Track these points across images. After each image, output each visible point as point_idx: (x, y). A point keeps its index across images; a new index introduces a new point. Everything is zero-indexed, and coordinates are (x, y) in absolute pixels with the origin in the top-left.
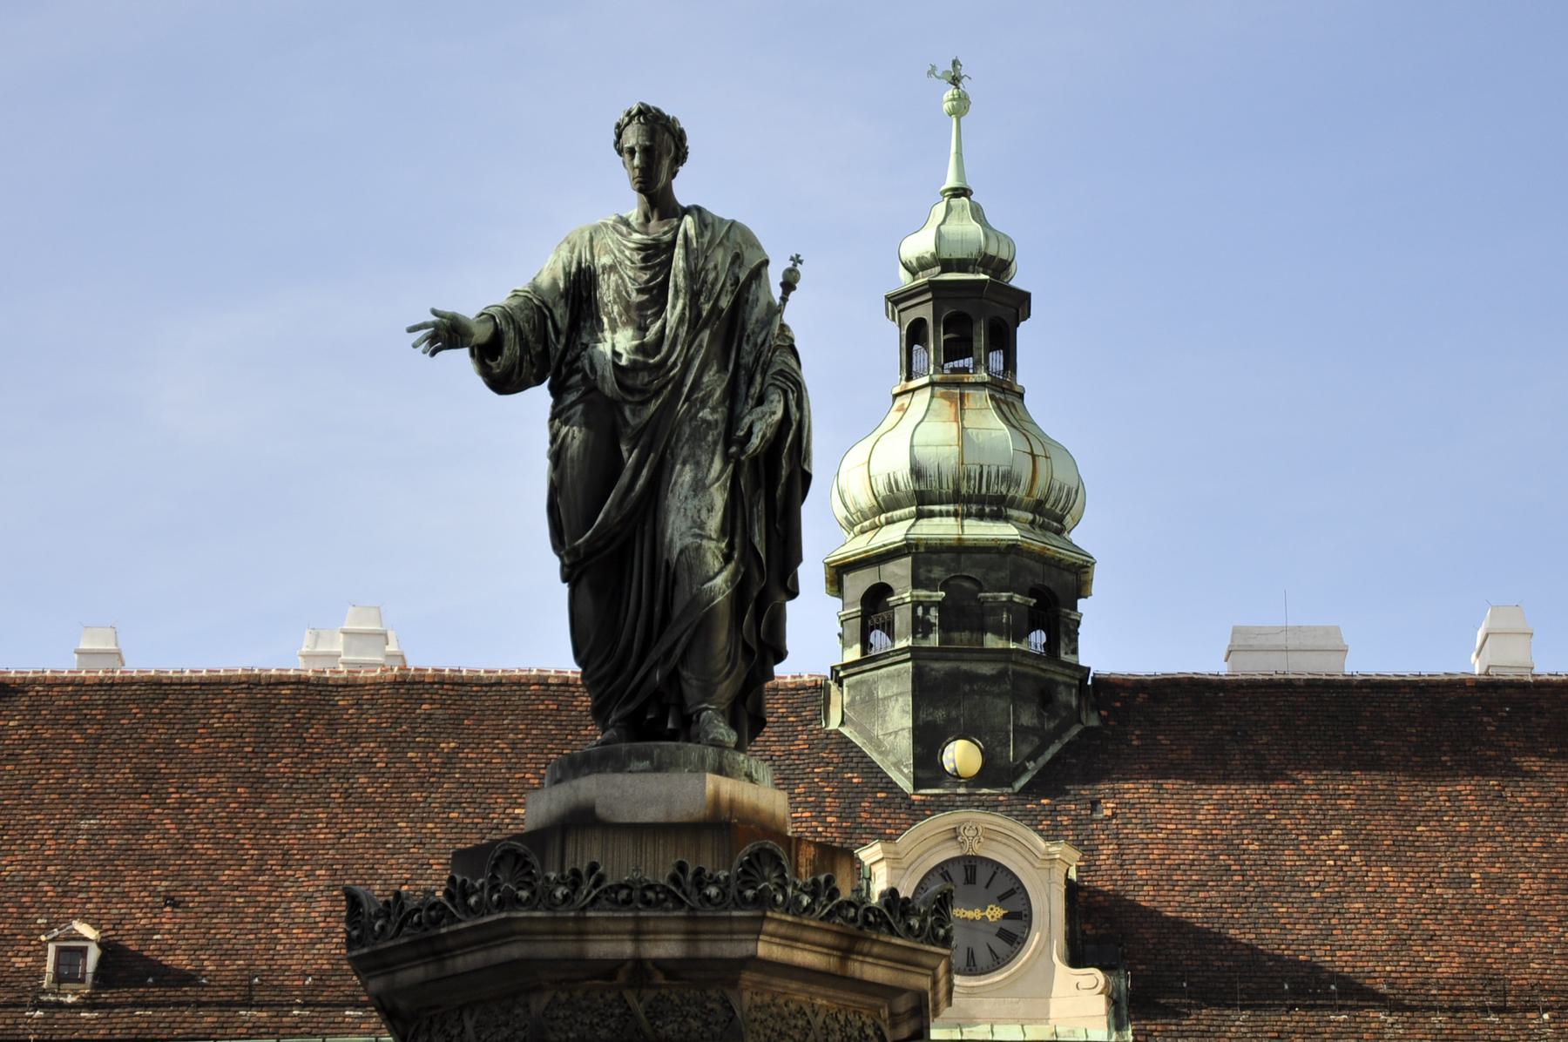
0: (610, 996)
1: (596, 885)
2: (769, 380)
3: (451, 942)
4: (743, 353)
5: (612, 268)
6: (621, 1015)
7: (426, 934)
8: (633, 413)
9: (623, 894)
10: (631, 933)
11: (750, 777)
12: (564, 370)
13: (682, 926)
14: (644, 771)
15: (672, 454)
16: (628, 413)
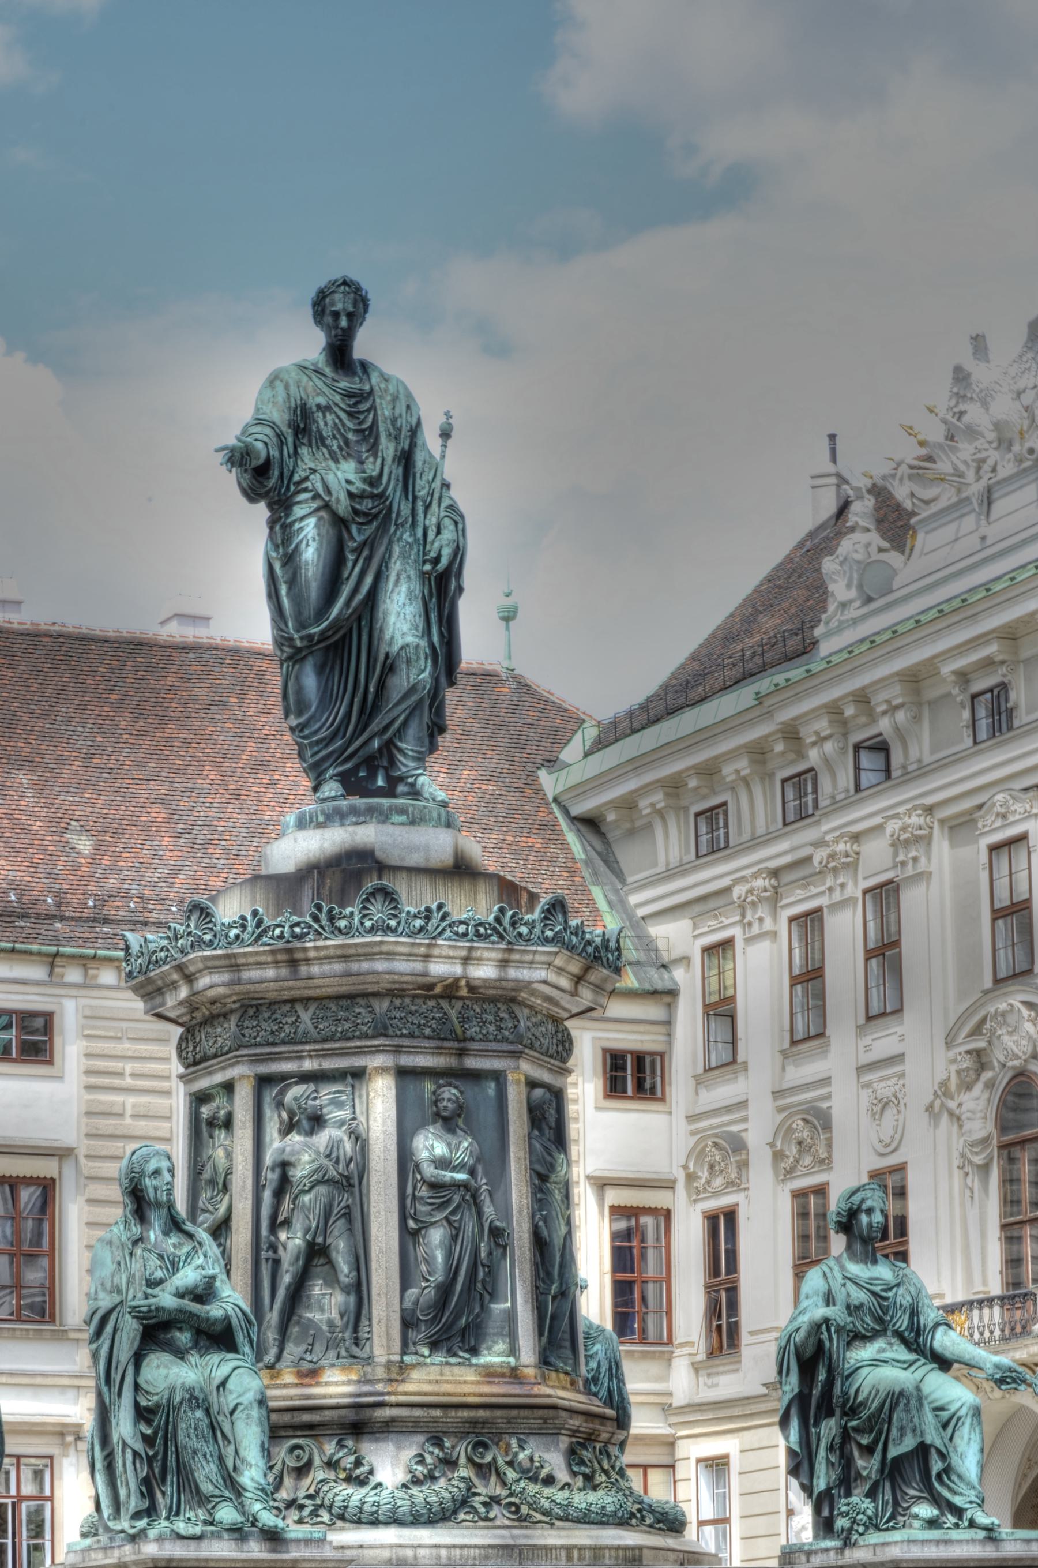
0: (431, 1003)
1: (443, 918)
3: (312, 954)
4: (417, 488)
5: (325, 409)
7: (290, 945)
8: (359, 531)
9: (462, 929)
10: (462, 959)
12: (292, 488)
14: (402, 824)
15: (387, 567)
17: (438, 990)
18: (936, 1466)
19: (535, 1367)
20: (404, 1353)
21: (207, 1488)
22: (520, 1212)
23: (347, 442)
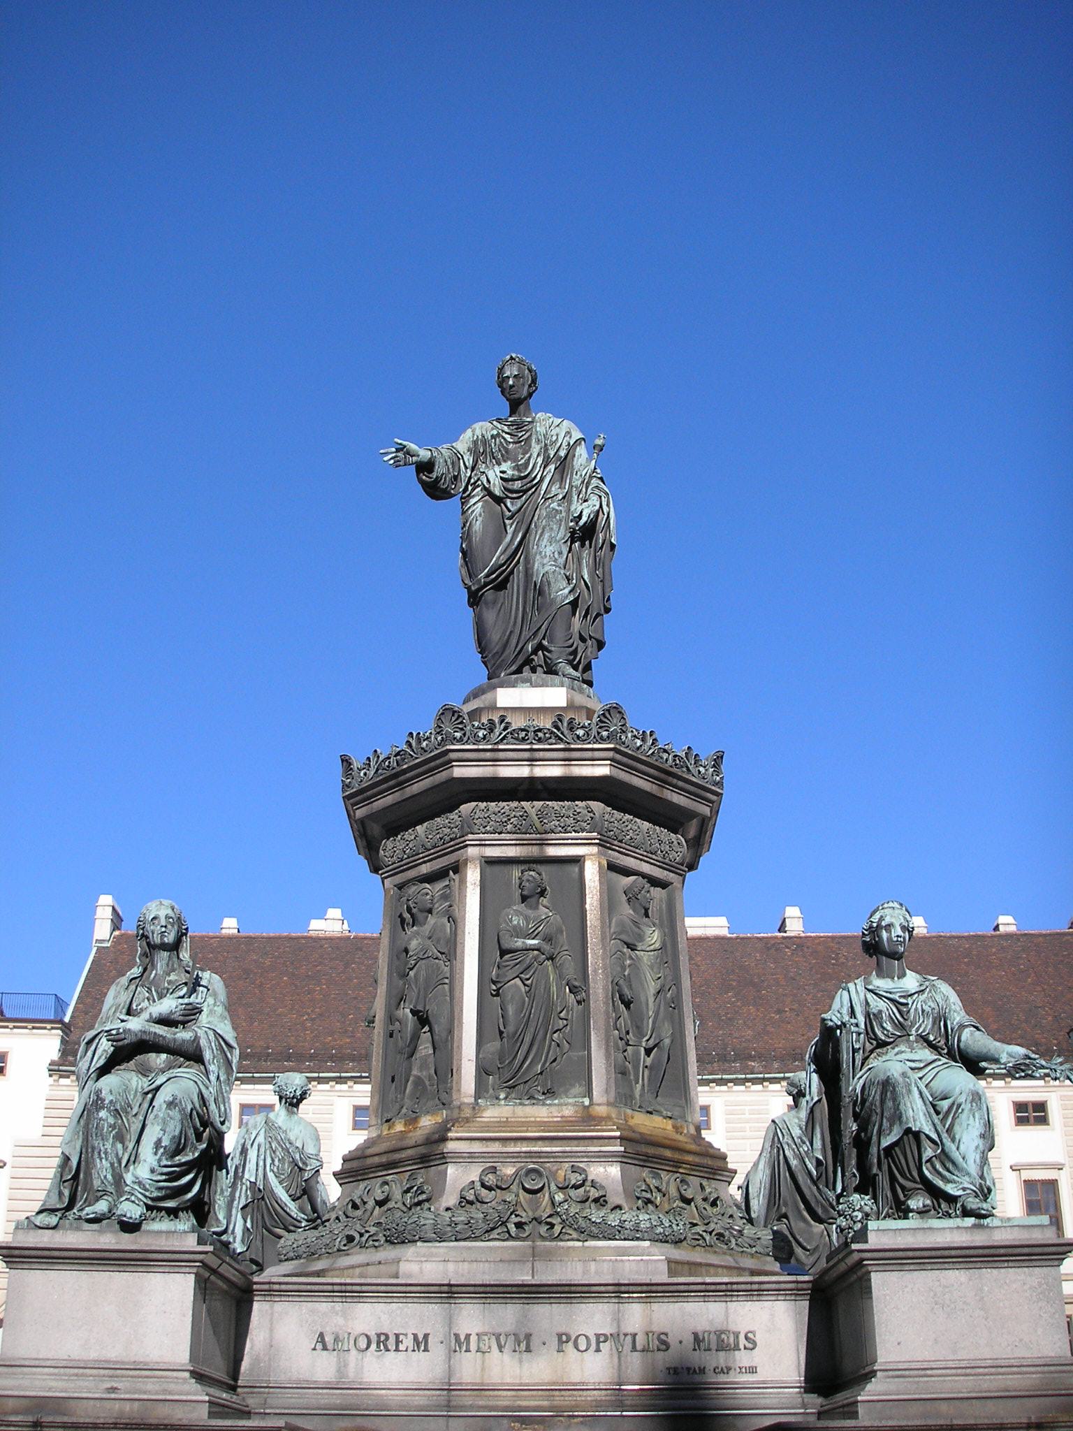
1: (505, 729)
2: (589, 491)
18: (928, 1152)
19: (609, 1104)
20: (478, 1094)
21: (97, 1183)
22: (595, 971)
23: (507, 451)
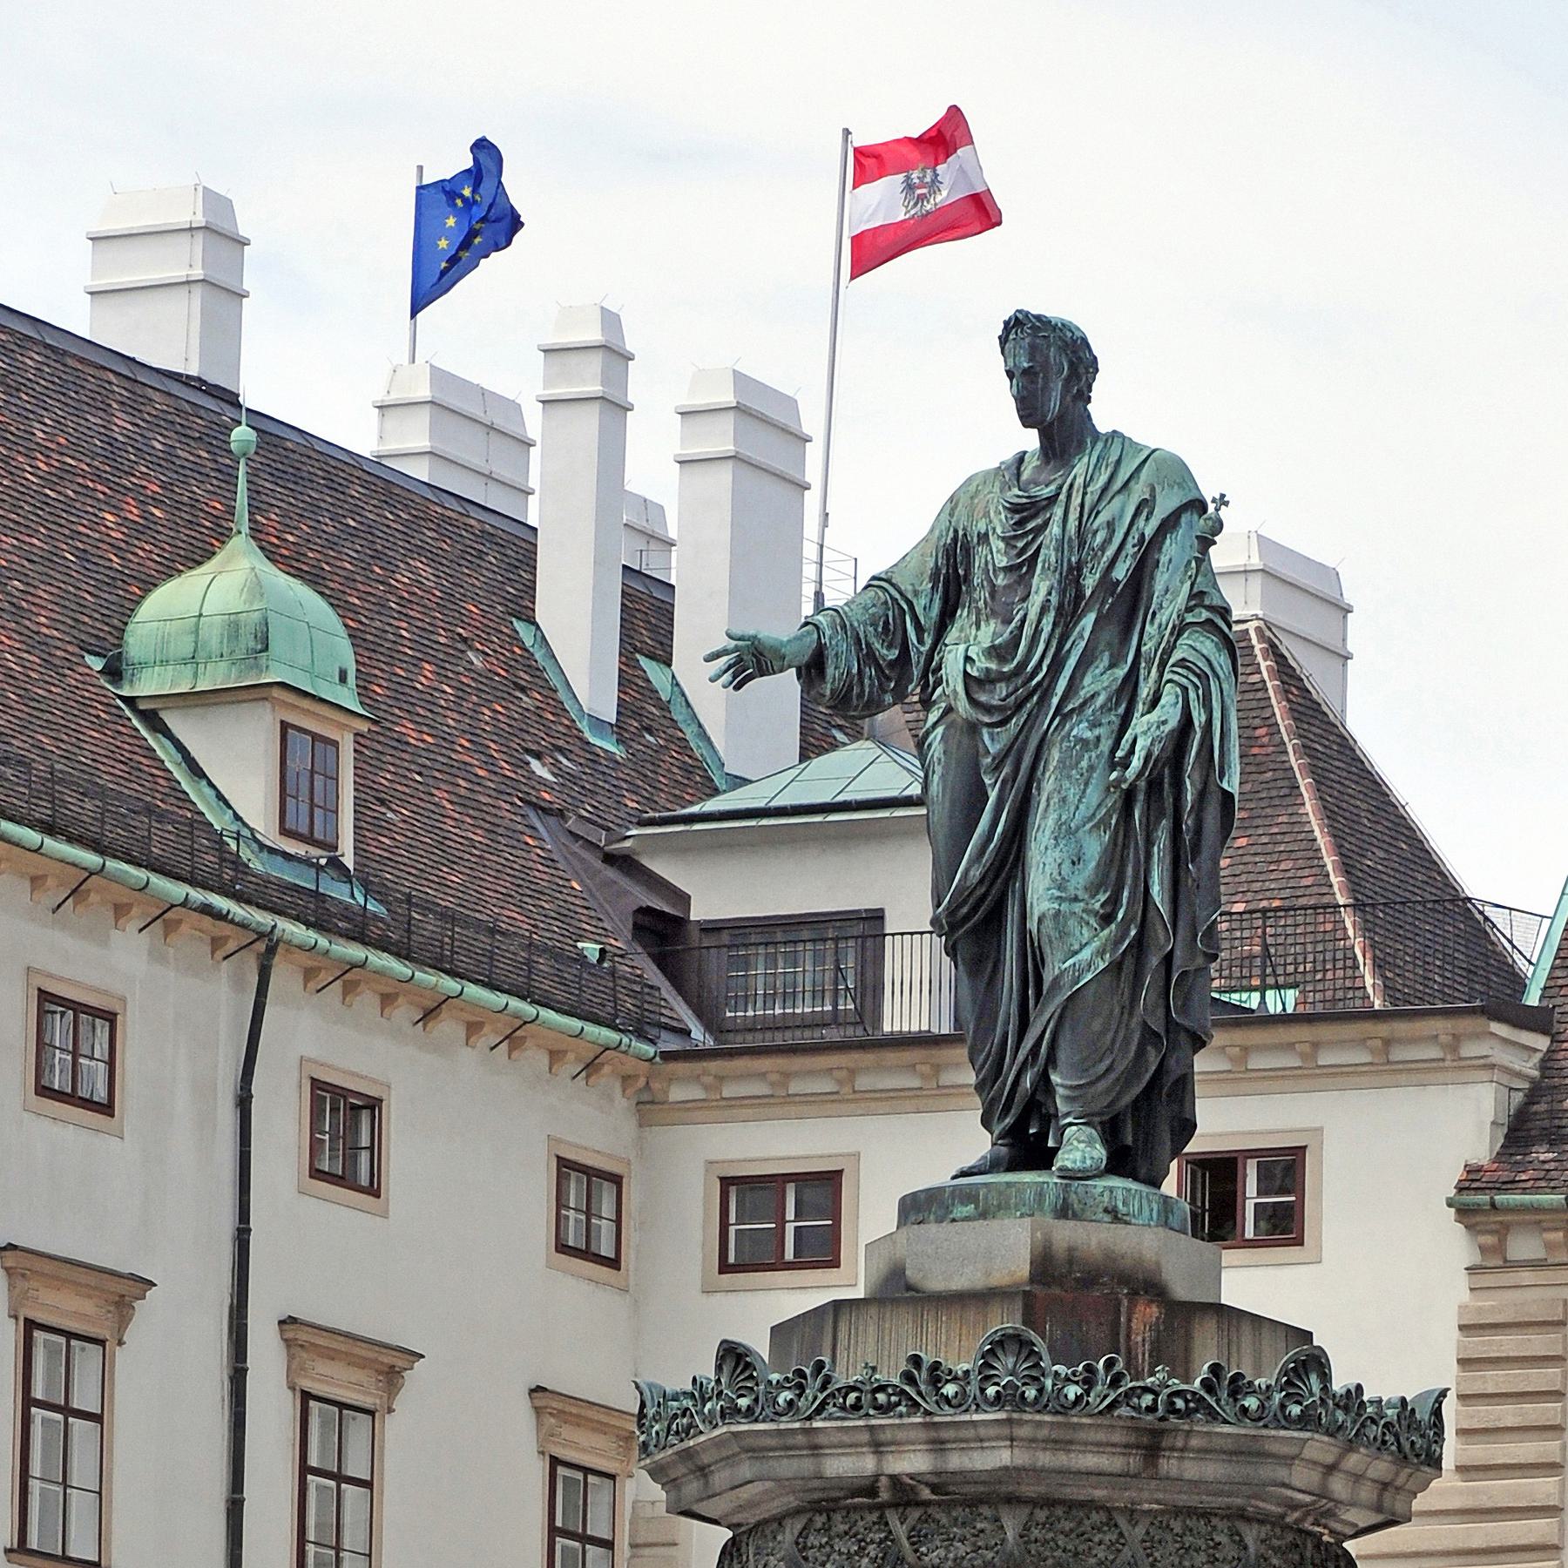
1: (823, 1388)
2: (1167, 676)
4: (1145, 638)
5: (984, 538)
6: (881, 1542)
11: (1114, 1215)
13: (922, 1435)
14: (967, 1219)
16: (986, 738)
17: (884, 1496)
